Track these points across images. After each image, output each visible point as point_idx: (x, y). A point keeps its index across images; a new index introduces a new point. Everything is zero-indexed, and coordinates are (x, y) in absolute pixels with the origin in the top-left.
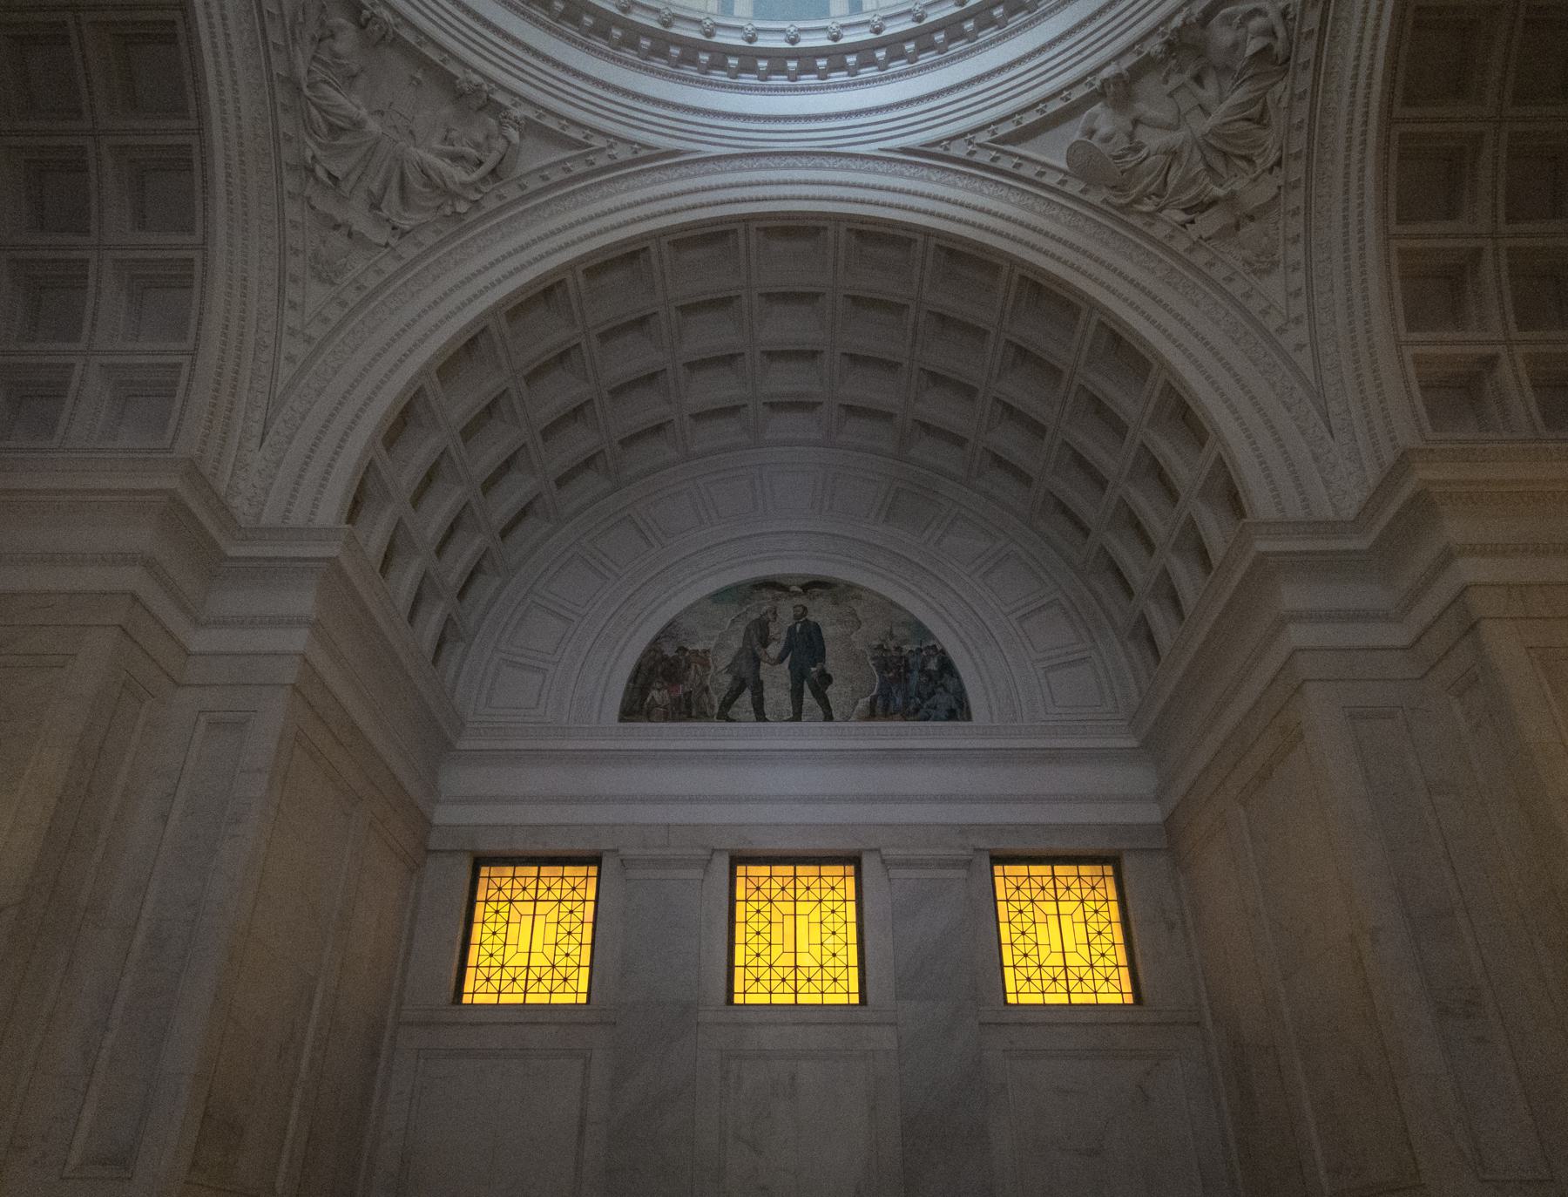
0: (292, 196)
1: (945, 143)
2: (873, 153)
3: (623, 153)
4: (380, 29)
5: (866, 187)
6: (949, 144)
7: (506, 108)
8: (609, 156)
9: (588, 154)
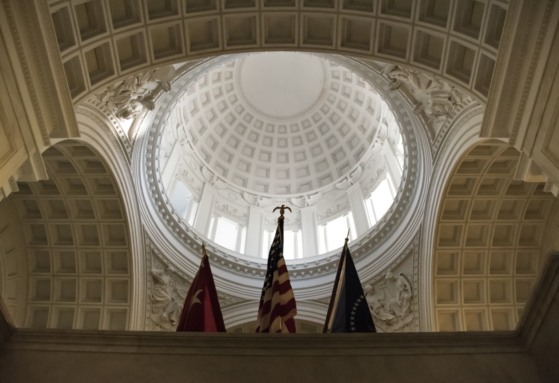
0: (148, 318)
3: (234, 301)
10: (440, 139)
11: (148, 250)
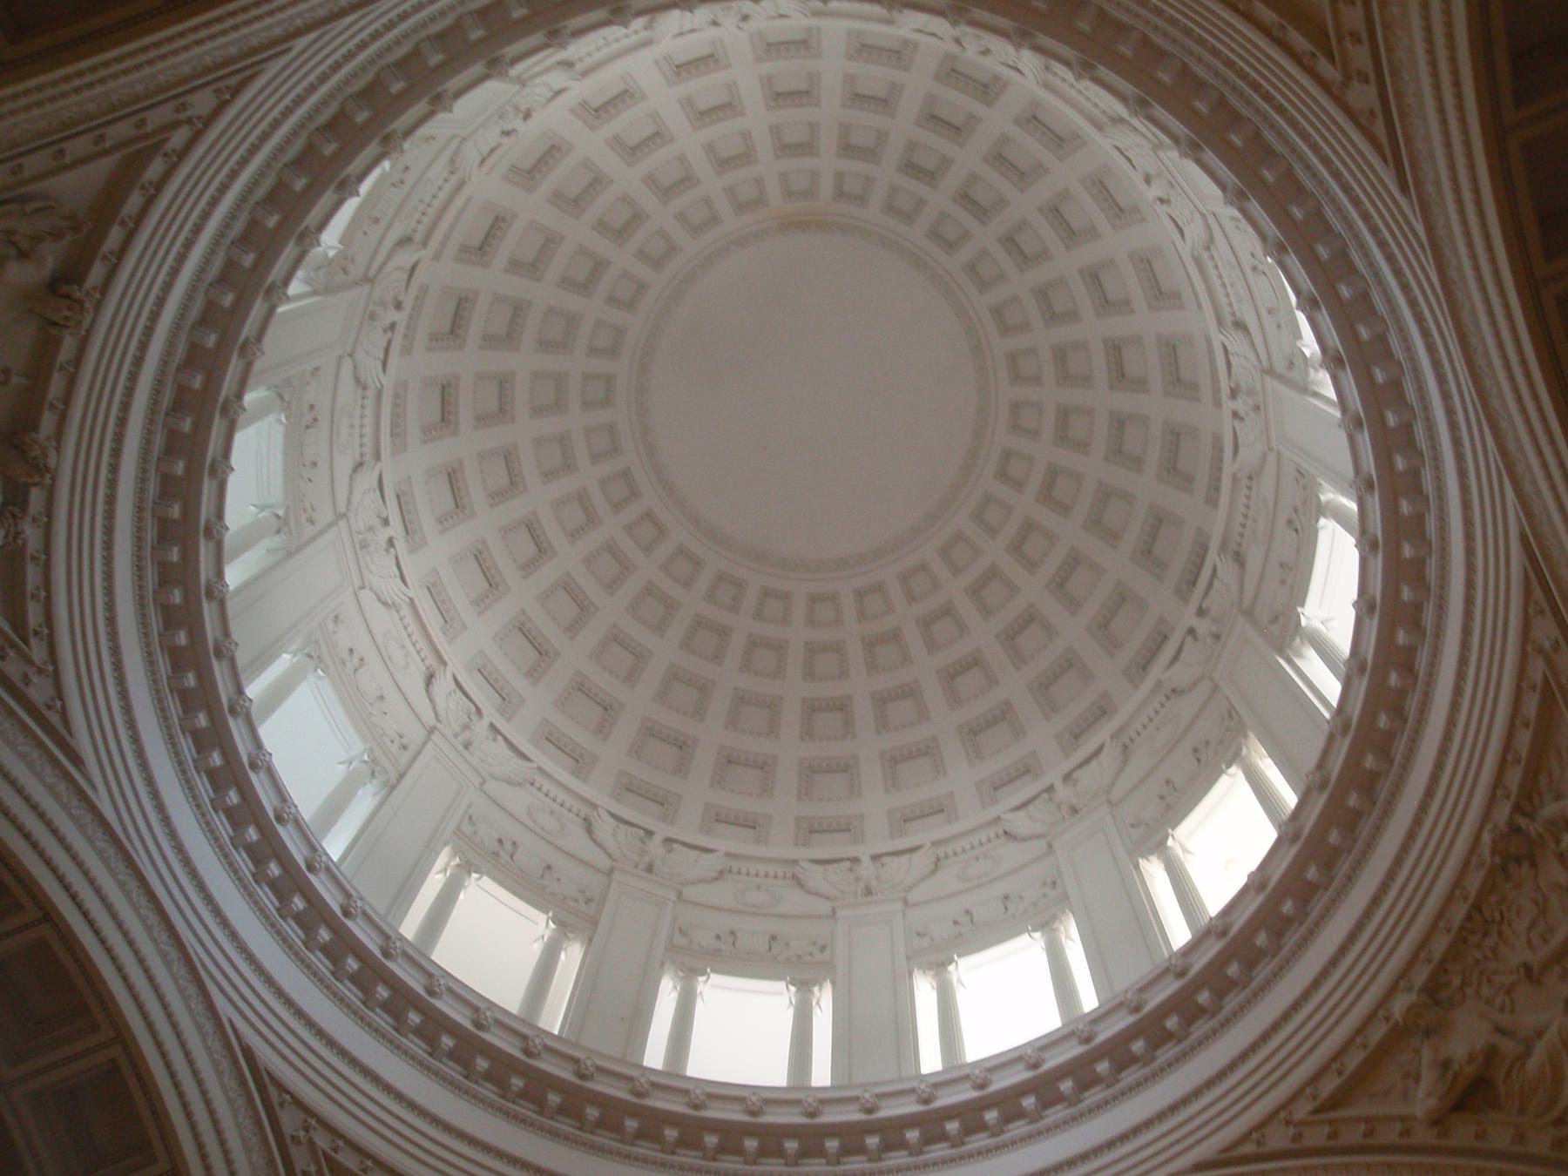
1: (288, 1097)
2: (225, 1021)
3: (39, 692)
4: (67, 318)
5: (183, 1044)
6: (290, 1103)
7: (24, 510)
8: (26, 676)
9: (13, 645)
10: (1353, 1136)
11: (156, 118)
